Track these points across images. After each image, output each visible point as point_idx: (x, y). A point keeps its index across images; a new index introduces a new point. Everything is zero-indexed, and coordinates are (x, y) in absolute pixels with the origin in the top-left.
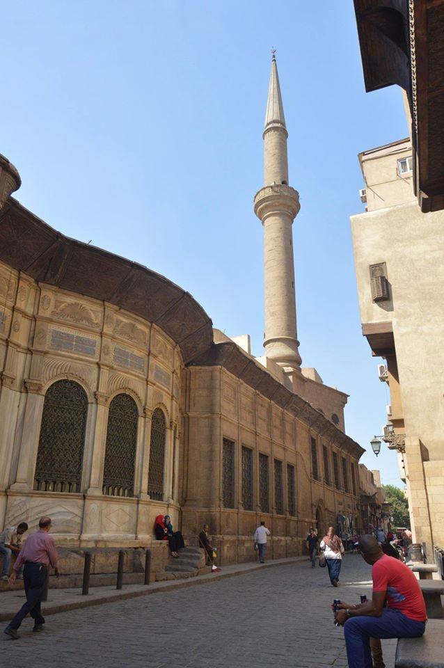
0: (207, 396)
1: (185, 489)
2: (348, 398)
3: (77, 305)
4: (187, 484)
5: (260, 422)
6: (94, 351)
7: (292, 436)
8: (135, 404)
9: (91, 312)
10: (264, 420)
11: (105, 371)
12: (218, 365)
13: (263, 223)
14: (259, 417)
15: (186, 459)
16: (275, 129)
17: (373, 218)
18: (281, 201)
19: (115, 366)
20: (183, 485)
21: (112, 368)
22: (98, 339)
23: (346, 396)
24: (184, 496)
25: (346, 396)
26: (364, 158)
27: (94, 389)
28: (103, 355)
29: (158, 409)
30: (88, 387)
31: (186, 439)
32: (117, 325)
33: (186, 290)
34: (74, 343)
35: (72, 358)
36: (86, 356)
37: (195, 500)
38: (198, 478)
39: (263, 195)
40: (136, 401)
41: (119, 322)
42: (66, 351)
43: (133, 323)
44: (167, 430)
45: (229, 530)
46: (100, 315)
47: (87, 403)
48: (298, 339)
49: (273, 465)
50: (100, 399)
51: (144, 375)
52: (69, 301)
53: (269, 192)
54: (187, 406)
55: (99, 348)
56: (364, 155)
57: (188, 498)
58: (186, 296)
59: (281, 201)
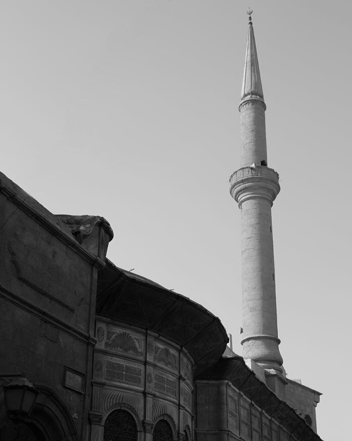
3: (124, 334)
6: (140, 379)
8: (170, 428)
9: (135, 340)
11: (150, 399)
12: (226, 380)
13: (240, 205)
16: (253, 101)
18: (261, 184)
19: (157, 394)
21: (154, 396)
22: (142, 367)
25: (320, 394)
27: (142, 418)
28: (147, 384)
29: (162, 421)
30: (137, 415)
32: (156, 352)
33: (216, 315)
34: (124, 373)
35: (124, 388)
36: (135, 385)
39: (240, 176)
40: (172, 428)
41: (158, 348)
42: (119, 382)
43: (168, 348)
46: (143, 343)
47: (136, 431)
48: (279, 338)
50: (148, 428)
51: (176, 399)
52: (118, 332)
53: (248, 174)
55: (144, 376)
58: (216, 321)
59: (261, 184)
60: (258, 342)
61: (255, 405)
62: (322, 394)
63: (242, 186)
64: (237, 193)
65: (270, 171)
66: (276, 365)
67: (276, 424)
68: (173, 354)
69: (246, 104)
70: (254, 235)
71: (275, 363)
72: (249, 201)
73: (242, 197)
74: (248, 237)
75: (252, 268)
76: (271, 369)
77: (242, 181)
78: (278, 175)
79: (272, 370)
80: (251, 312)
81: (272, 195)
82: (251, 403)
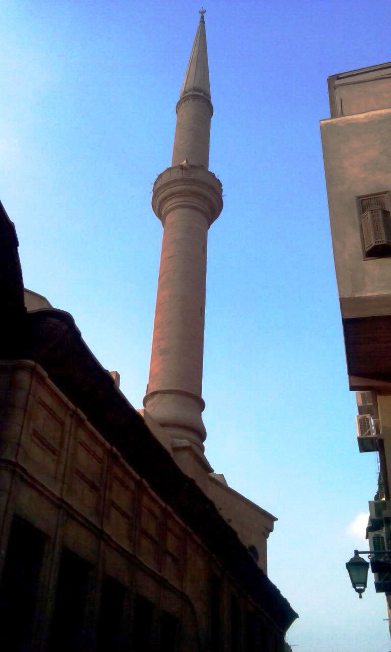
2: (275, 523)
5: (114, 514)
7: (175, 560)
10: (124, 514)
14: (113, 504)
16: (195, 97)
17: (365, 124)
18: (194, 188)
23: (272, 519)
25: (272, 519)
26: (337, 82)
53: (177, 175)
56: (339, 79)
59: (194, 188)
60: (169, 398)
61: (122, 460)
62: (277, 519)
63: (168, 191)
66: (194, 437)
67: (177, 522)
69: (185, 101)
72: (175, 211)
73: (168, 205)
75: (170, 296)
76: (184, 439)
77: (168, 184)
78: (221, 185)
79: (185, 441)
82: (112, 450)
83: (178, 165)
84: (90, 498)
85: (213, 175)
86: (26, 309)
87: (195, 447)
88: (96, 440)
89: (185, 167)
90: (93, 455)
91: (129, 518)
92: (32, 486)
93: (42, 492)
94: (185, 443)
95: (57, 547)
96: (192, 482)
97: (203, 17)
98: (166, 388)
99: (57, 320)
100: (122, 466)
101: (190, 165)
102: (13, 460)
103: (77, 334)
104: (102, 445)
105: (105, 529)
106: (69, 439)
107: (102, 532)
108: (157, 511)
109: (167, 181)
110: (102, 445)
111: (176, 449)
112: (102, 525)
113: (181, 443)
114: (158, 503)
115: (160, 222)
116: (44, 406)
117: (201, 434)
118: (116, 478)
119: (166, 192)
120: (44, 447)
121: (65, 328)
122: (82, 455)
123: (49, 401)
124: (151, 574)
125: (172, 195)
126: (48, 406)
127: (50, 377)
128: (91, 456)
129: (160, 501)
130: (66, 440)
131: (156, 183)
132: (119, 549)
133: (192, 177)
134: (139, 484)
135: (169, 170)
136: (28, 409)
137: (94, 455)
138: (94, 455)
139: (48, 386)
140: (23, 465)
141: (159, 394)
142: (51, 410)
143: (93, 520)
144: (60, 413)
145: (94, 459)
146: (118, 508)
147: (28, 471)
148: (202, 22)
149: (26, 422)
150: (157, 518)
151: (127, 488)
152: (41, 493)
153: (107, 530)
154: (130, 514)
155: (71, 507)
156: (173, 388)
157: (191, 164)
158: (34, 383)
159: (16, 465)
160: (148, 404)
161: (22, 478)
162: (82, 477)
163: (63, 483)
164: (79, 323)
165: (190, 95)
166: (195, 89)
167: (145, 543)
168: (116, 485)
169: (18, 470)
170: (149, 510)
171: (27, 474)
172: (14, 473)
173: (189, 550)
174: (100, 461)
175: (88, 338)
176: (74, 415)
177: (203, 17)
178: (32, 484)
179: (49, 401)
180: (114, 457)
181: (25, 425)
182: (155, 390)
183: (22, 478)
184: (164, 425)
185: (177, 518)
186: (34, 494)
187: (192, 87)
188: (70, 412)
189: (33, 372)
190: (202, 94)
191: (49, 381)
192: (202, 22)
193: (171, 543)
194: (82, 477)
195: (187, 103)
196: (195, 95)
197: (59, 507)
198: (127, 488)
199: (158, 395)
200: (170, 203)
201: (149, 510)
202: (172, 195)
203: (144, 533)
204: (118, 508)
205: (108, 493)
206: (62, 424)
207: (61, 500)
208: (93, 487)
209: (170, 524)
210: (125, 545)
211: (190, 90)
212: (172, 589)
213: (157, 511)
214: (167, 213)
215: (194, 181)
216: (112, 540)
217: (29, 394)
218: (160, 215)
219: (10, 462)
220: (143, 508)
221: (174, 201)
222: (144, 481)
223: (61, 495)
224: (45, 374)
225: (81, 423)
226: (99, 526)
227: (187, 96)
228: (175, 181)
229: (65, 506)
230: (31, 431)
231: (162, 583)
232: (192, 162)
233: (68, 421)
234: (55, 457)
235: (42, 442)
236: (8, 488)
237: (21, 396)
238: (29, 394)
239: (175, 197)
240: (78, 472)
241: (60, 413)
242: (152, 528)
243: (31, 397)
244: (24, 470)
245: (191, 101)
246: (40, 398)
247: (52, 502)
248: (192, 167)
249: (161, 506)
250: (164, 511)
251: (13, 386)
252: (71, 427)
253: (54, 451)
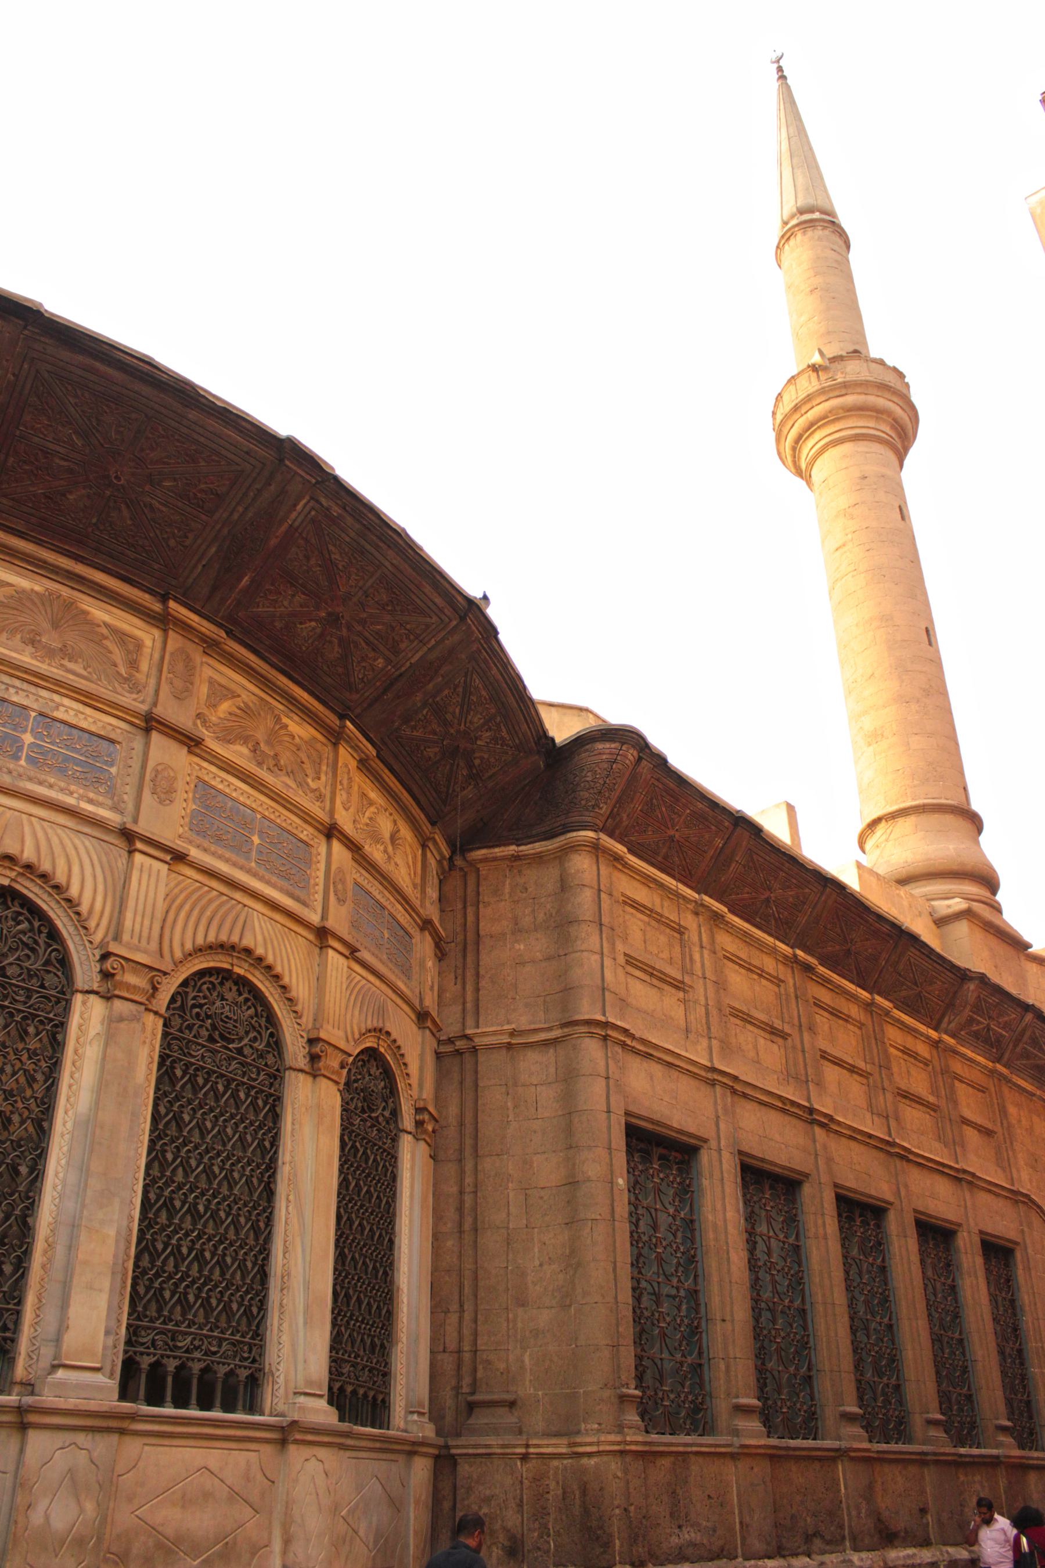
0: (549, 959)
1: (467, 1356)
4: (475, 1334)
5: (832, 1074)
7: (987, 1133)
10: (852, 1069)
14: (824, 1055)
15: (467, 1226)
16: (807, 225)
18: (850, 399)
20: (460, 1340)
24: (466, 1389)
31: (469, 1142)
33: (281, 425)
37: (512, 1404)
38: (522, 1303)
43: (65, 592)
44: (290, 1077)
45: (689, 1535)
49: (912, 1243)
53: (809, 385)
54: (469, 1006)
57: (479, 1397)
63: (801, 422)
64: (794, 449)
65: (874, 365)
67: (971, 1060)
68: (107, 625)
69: (788, 239)
70: (850, 536)
71: (967, 881)
73: (807, 450)
74: (837, 545)
75: (857, 625)
76: (953, 898)
77: (796, 408)
78: (901, 375)
79: (958, 900)
80: (870, 745)
81: (893, 427)
82: (795, 956)
83: (805, 366)
84: (771, 1053)
85: (881, 362)
86: (553, 740)
87: (977, 907)
88: (761, 946)
89: (820, 366)
90: (758, 974)
91: (864, 1074)
92: (648, 1056)
93: (672, 1063)
94: (957, 904)
95: (726, 1155)
96: (982, 979)
97: (780, 69)
98: (895, 808)
99: (613, 746)
100: (825, 982)
101: (829, 359)
102: (599, 1017)
103: (660, 761)
104: (773, 952)
105: (816, 1106)
106: (702, 956)
107: (811, 1111)
108: (923, 1050)
109: (793, 404)
110: (773, 952)
111: (941, 922)
112: (809, 1100)
113: (949, 906)
114: (922, 1034)
115: (804, 483)
116: (631, 906)
117: (989, 882)
118: (818, 1004)
119: (796, 425)
120: (655, 982)
121: (632, 754)
122: (737, 979)
123: (641, 894)
124: (938, 1169)
125: (811, 427)
126: (644, 906)
127: (630, 851)
128: (756, 977)
129: (922, 1028)
130: (697, 957)
131: (774, 413)
132: (856, 1136)
133: (839, 380)
134: (869, 1007)
135: (792, 380)
136: (605, 920)
137: (762, 974)
138: (762, 974)
139: (631, 868)
140: (619, 1023)
141: (883, 823)
142: (651, 910)
143: (789, 1092)
144: (669, 912)
145: (764, 982)
146: (838, 1063)
147: (632, 1031)
148: (782, 77)
149: (605, 944)
150: (926, 1063)
151: (847, 1019)
152: (670, 1065)
153: (824, 1105)
154: (861, 1064)
155: (735, 1078)
156: (910, 803)
157: (831, 356)
158: (604, 870)
159: (606, 1025)
160: (868, 846)
161: (624, 1045)
162: (747, 1019)
163: (710, 1038)
164: (656, 740)
165: (797, 225)
166: (801, 212)
167: (913, 1115)
168: (822, 1020)
169: (610, 1032)
170: (905, 1051)
171: (633, 1037)
172: (605, 1038)
173: (1012, 1110)
174: (778, 981)
175: (677, 760)
176: (699, 909)
177: (780, 69)
178: (648, 1052)
179: (641, 894)
180: (808, 968)
181: (605, 951)
182: (874, 816)
183: (624, 1045)
184: (904, 881)
185: (969, 1053)
186: (657, 1069)
187: (794, 210)
188: (691, 906)
189: (596, 848)
190: (817, 215)
191: (632, 859)
192: (782, 77)
193: (969, 1104)
194: (747, 1019)
195: (792, 242)
196: (806, 222)
197: (713, 1083)
198: (847, 1019)
199: (883, 824)
200: (811, 442)
201: (905, 1051)
202: (811, 427)
203: (905, 1095)
204: (838, 1063)
205: (806, 1036)
206: (680, 930)
207: (714, 1070)
208: (774, 1032)
209: (957, 1067)
210: (870, 1125)
211: (792, 217)
212: (992, 1189)
213: (923, 1050)
214: (811, 464)
215: (846, 387)
216: (839, 1123)
217: (599, 890)
218: (803, 473)
219: (588, 1022)
220: (892, 1050)
221: (817, 436)
222: (878, 999)
223: (711, 1060)
224: (620, 849)
225: (716, 918)
226: (806, 1104)
227: (790, 229)
228: (809, 398)
229: (725, 1080)
230: (621, 960)
231: (961, 1178)
232: (831, 351)
233: (689, 921)
234: (681, 994)
235: (652, 975)
236: (602, 1070)
237: (585, 898)
238: (599, 890)
239: (819, 428)
240: (737, 1014)
241: (669, 912)
242: (919, 1083)
243: (603, 895)
244: (625, 1031)
245: (799, 236)
246: (623, 895)
247: (694, 1076)
248: (833, 360)
249: (928, 1037)
250: (936, 1044)
251: (564, 886)
252: (700, 933)
253: (678, 986)
